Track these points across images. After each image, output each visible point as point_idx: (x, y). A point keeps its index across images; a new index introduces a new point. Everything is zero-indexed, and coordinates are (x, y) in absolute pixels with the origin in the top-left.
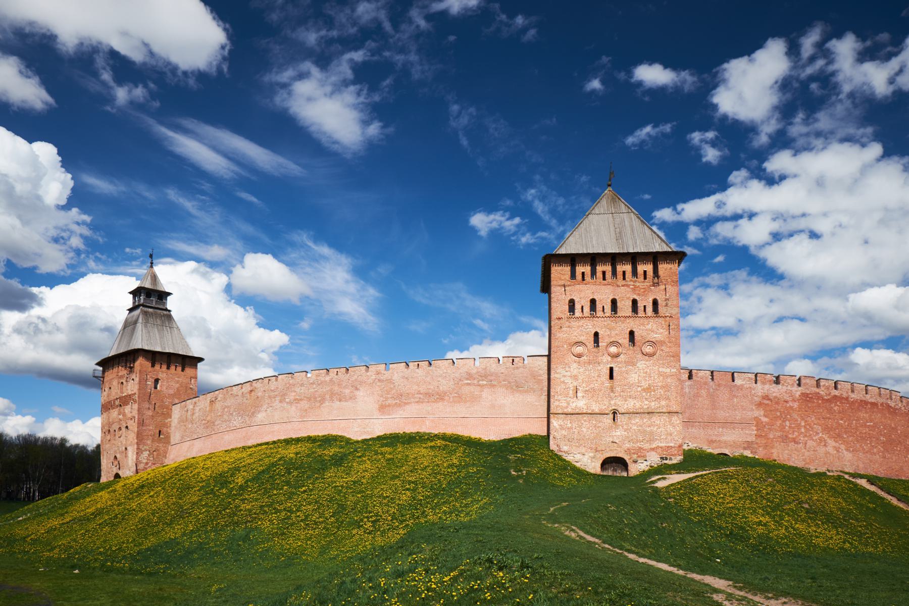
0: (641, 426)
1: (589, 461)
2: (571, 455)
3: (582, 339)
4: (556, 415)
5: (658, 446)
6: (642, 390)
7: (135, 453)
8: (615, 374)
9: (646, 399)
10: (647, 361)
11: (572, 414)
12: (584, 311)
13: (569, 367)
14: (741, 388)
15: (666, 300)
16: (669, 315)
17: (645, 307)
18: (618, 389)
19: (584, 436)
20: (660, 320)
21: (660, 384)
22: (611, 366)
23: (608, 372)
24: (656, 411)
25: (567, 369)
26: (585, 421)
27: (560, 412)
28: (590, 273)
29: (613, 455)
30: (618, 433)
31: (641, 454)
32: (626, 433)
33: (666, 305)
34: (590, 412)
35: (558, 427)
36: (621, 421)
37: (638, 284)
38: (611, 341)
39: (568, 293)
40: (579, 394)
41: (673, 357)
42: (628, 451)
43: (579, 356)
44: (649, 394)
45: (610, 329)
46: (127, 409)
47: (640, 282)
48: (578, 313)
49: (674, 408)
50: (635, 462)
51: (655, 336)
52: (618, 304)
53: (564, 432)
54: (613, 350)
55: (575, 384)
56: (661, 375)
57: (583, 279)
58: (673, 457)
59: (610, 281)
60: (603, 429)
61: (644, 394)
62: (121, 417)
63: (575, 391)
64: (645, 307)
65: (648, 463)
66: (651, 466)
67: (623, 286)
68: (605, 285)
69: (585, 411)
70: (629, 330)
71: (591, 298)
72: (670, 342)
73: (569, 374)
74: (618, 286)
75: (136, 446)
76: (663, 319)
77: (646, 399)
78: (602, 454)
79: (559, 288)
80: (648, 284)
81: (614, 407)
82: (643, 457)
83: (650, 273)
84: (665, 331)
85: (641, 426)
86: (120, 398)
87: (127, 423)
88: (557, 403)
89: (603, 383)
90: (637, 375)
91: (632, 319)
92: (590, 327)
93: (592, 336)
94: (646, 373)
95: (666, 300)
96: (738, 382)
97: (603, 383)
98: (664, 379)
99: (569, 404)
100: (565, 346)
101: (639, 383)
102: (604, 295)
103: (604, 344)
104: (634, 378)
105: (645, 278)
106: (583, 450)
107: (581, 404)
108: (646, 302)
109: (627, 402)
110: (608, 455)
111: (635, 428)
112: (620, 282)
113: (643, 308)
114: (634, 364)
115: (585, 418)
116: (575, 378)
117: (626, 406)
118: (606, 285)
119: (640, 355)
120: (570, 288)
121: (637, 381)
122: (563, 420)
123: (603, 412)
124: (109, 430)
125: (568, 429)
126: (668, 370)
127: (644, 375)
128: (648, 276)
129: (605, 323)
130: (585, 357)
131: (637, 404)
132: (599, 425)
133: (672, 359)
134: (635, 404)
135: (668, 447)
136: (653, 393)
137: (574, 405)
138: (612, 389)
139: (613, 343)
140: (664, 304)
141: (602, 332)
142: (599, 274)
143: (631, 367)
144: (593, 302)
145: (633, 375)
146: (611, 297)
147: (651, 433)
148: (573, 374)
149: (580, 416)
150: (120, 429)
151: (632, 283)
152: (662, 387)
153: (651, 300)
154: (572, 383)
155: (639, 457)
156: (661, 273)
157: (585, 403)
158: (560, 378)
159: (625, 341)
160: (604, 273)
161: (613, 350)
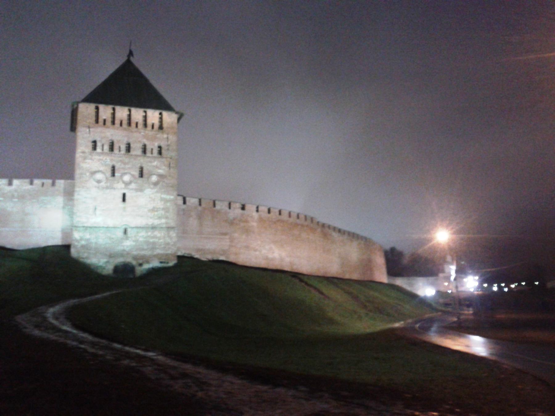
3: (102, 168)
14: (218, 212)
17: (152, 149)
20: (164, 160)
33: (168, 149)
37: (147, 132)
39: (92, 134)
40: (98, 212)
42: (135, 258)
43: (99, 182)
47: (149, 132)
64: (152, 149)
70: (139, 165)
74: (132, 132)
96: (218, 207)
112: (135, 129)
116: (95, 199)
138: (124, 209)
139: (125, 174)
140: (166, 148)
147: (154, 243)
151: (142, 131)
152: (163, 209)
153: (156, 144)
159: (136, 173)
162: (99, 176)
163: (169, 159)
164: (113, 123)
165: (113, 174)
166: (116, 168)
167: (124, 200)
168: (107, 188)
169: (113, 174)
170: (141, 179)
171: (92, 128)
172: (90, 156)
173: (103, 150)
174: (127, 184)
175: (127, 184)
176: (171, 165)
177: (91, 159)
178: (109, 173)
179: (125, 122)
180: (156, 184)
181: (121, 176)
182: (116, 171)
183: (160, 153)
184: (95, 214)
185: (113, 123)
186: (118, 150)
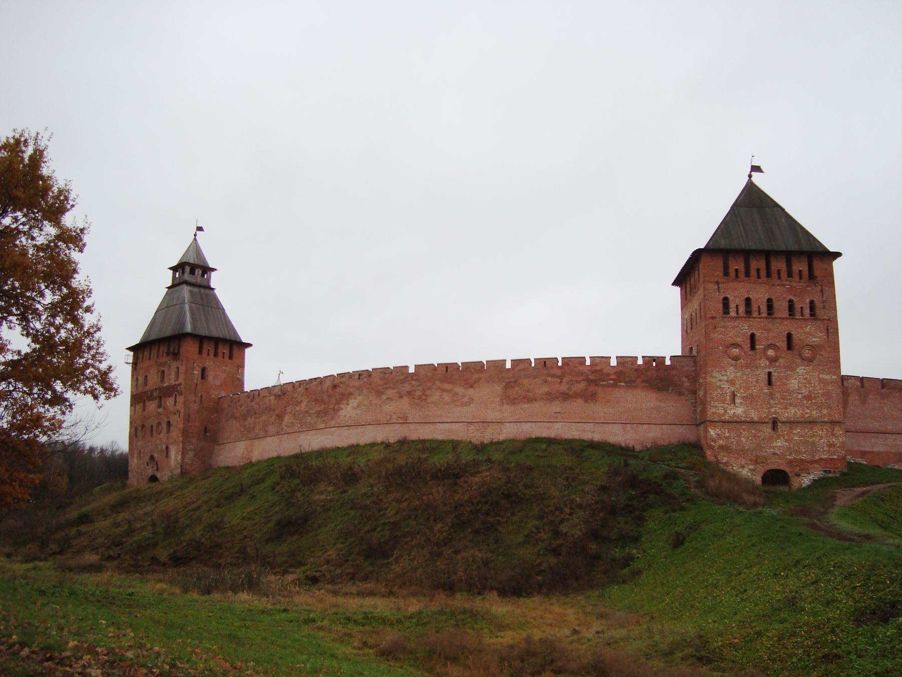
0: (802, 436)
2: (730, 467)
4: (713, 424)
6: (803, 397)
7: (180, 453)
8: (773, 379)
9: (807, 407)
10: (807, 366)
12: (740, 312)
18: (778, 395)
19: (743, 447)
21: (820, 391)
22: (770, 370)
23: (766, 377)
26: (744, 430)
27: (716, 420)
30: (780, 444)
31: (803, 466)
34: (749, 420)
35: (714, 436)
36: (781, 431)
38: (769, 343)
40: (738, 401)
41: (834, 362)
42: (790, 462)
43: (736, 359)
45: (768, 330)
46: (169, 402)
48: (733, 313)
49: (837, 417)
50: (798, 475)
51: (814, 339)
52: (775, 305)
53: (721, 442)
54: (771, 353)
55: (733, 389)
57: (737, 276)
59: (765, 279)
60: (764, 440)
61: (805, 402)
62: (161, 410)
63: (732, 397)
65: (811, 477)
66: (814, 480)
67: (778, 285)
68: (758, 284)
69: (743, 419)
71: (746, 296)
73: (725, 378)
74: (773, 285)
75: (181, 445)
77: (807, 407)
79: (711, 285)
80: (805, 284)
81: (774, 416)
84: (823, 334)
85: (802, 436)
86: (159, 389)
87: (168, 418)
88: (713, 410)
89: (762, 389)
91: (789, 321)
92: (747, 328)
94: (806, 379)
95: (823, 302)
97: (762, 389)
99: (726, 411)
101: (798, 389)
102: (760, 294)
104: (794, 384)
105: (801, 278)
106: (743, 462)
107: (739, 411)
108: (803, 303)
110: (769, 468)
111: (797, 438)
112: (775, 281)
113: (800, 310)
115: (744, 427)
116: (732, 382)
118: (760, 283)
119: (799, 361)
120: (724, 285)
121: (797, 388)
123: (763, 421)
124: (143, 426)
125: (727, 438)
126: (828, 377)
129: (762, 324)
131: (798, 412)
132: (759, 435)
133: (832, 364)
134: (795, 412)
136: (814, 401)
137: (732, 412)
138: (771, 396)
139: (770, 346)
140: (821, 305)
142: (753, 272)
143: (790, 373)
144: (748, 301)
146: (767, 296)
147: (814, 444)
149: (739, 425)
150: (159, 424)
151: (787, 283)
152: (823, 395)
154: (729, 388)
155: (801, 470)
156: (817, 273)
157: (743, 410)
158: (716, 383)
159: (783, 344)
160: (758, 270)
161: (771, 353)
163: (826, 321)
164: (747, 274)
165: (753, 347)
167: (770, 383)
168: (747, 366)
169: (753, 347)
170: (790, 352)
172: (722, 324)
175: (773, 360)
176: (831, 330)
177: (724, 327)
178: (747, 347)
179: (763, 273)
180: (810, 360)
181: (765, 350)
182: (757, 343)
183: (813, 314)
184: (734, 403)
185: (747, 274)
186: (757, 313)
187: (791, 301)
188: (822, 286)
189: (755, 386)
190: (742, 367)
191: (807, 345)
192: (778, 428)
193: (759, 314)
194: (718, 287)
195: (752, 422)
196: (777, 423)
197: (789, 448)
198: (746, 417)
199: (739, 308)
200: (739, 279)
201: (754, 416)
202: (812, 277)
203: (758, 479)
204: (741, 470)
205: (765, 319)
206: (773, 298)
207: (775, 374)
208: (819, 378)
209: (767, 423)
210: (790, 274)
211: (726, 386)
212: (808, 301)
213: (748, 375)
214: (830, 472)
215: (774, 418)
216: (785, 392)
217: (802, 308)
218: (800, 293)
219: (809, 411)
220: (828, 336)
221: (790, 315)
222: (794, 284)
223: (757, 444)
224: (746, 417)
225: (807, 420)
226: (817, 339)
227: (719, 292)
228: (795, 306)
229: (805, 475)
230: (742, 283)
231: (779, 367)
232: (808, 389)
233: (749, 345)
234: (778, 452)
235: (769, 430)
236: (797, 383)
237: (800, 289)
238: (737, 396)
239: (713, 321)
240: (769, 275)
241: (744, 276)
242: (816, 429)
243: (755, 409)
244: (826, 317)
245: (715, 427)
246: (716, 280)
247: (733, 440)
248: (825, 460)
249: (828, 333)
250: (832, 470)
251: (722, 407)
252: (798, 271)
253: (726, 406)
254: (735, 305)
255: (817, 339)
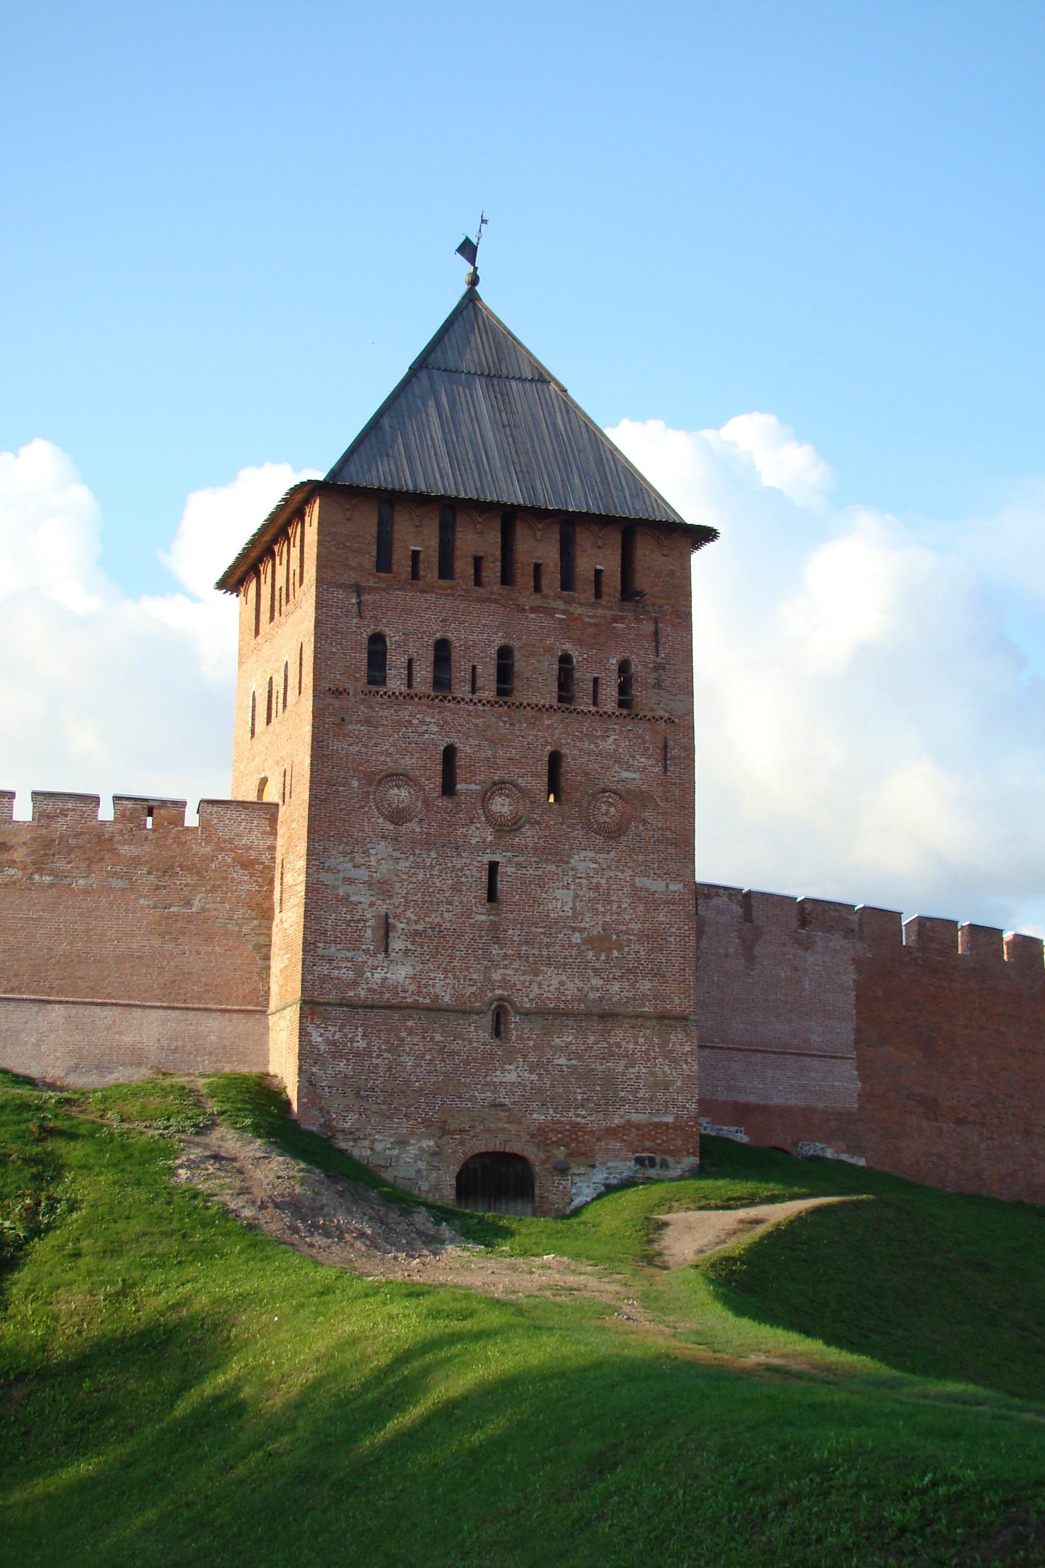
1: (421, 1165)
2: (367, 1143)
3: (408, 762)
4: (321, 1009)
5: (628, 1122)
6: (585, 941)
8: (501, 886)
11: (372, 1007)
12: (417, 679)
13: (366, 853)
15: (659, 667)
16: (666, 715)
17: (596, 680)
18: (514, 933)
19: (407, 1082)
20: (640, 728)
21: (636, 927)
22: (497, 858)
23: (485, 876)
24: (622, 1010)
25: (359, 859)
26: (410, 1032)
28: (435, 559)
29: (494, 1145)
30: (512, 1077)
32: (534, 1077)
34: (428, 1001)
35: (323, 1047)
36: (518, 1037)
40: (397, 944)
42: (539, 1135)
43: (398, 817)
44: (603, 958)
45: (494, 743)
48: (395, 683)
49: (677, 1003)
50: (563, 1171)
51: (625, 775)
52: (520, 665)
54: (501, 806)
55: (383, 908)
56: (640, 899)
57: (415, 575)
58: (670, 1159)
59: (497, 588)
61: (590, 954)
63: (382, 933)
67: (533, 610)
68: (478, 600)
69: (410, 1000)
71: (438, 635)
72: (666, 800)
73: (362, 874)
74: (521, 609)
76: (648, 725)
78: (462, 1143)
79: (340, 594)
80: (609, 613)
81: (498, 992)
82: (585, 1154)
83: (613, 580)
85: (579, 1056)
89: (468, 913)
90: (571, 893)
92: (435, 729)
93: (439, 757)
94: (597, 887)
95: (655, 669)
97: (468, 913)
98: (647, 911)
99: (359, 972)
100: (355, 784)
101: (574, 917)
103: (473, 787)
105: (598, 594)
107: (400, 973)
109: (539, 979)
110: (481, 1145)
111: (562, 1061)
112: (528, 599)
113: (590, 685)
114: (562, 860)
115: (410, 1023)
116: (382, 888)
117: (536, 990)
119: (579, 833)
121: (570, 914)
122: (342, 1027)
123: (468, 1007)
125: (357, 1054)
126: (659, 886)
127: (592, 894)
128: (605, 589)
129: (479, 721)
130: (414, 825)
131: (570, 985)
132: (454, 1047)
135: (657, 1125)
136: (615, 953)
137: (378, 976)
138: (496, 934)
139: (498, 787)
140: (651, 681)
141: (468, 750)
142: (463, 567)
143: (553, 868)
144: (442, 650)
145: (559, 893)
146: (499, 641)
147: (610, 1081)
148: (377, 876)
151: (560, 604)
152: (643, 937)
154: (372, 904)
156: (643, 581)
157: (411, 972)
158: (335, 887)
159: (541, 784)
160: (478, 561)
161: (501, 806)
162: (401, 795)
163: (662, 724)
164: (446, 571)
165: (448, 788)
166: (461, 761)
167: (492, 896)
168: (428, 843)
169: (448, 788)
171: (372, 590)
173: (410, 685)
174: (507, 828)
175: (507, 828)
177: (368, 722)
178: (434, 783)
179: (492, 571)
180: (613, 833)
181: (485, 798)
184: (386, 951)
185: (446, 571)
187: (565, 660)
188: (656, 621)
189: (450, 903)
190: (414, 841)
191: (604, 791)
192: (508, 1030)
193: (473, 692)
194: (359, 604)
195: (435, 1009)
196: (506, 1012)
197: (540, 1090)
198: (419, 993)
199: (416, 667)
200: (420, 583)
201: (443, 989)
202: (628, 592)
203: (448, 1180)
204: (396, 1152)
205: (488, 708)
206: (515, 644)
207: (510, 870)
208: (633, 885)
209: (479, 1012)
210: (568, 582)
211: (362, 897)
212: (614, 661)
213: (432, 867)
214: (652, 1163)
215: (501, 999)
216: (535, 924)
217: (596, 680)
218: (595, 636)
219: (601, 982)
220: (665, 768)
221: (560, 699)
222: (579, 611)
223: (446, 1075)
224: (419, 993)
225: (595, 1011)
226: (633, 776)
227: (360, 615)
228: (577, 675)
229: (582, 1170)
230: (428, 596)
231: (522, 850)
232: (600, 919)
233: (439, 780)
234: (507, 1101)
235: (485, 1035)
236: (570, 899)
237: (596, 625)
238: (395, 927)
239: (337, 704)
240: (507, 578)
241: (436, 574)
242: (618, 1035)
243: (446, 971)
244: (662, 713)
245: (325, 1019)
246: (353, 582)
247: (375, 1061)
248: (638, 1127)
249: (665, 759)
250: (658, 1160)
251: (351, 960)
252: (593, 573)
253: (362, 958)
254: (404, 659)
255: (633, 776)
